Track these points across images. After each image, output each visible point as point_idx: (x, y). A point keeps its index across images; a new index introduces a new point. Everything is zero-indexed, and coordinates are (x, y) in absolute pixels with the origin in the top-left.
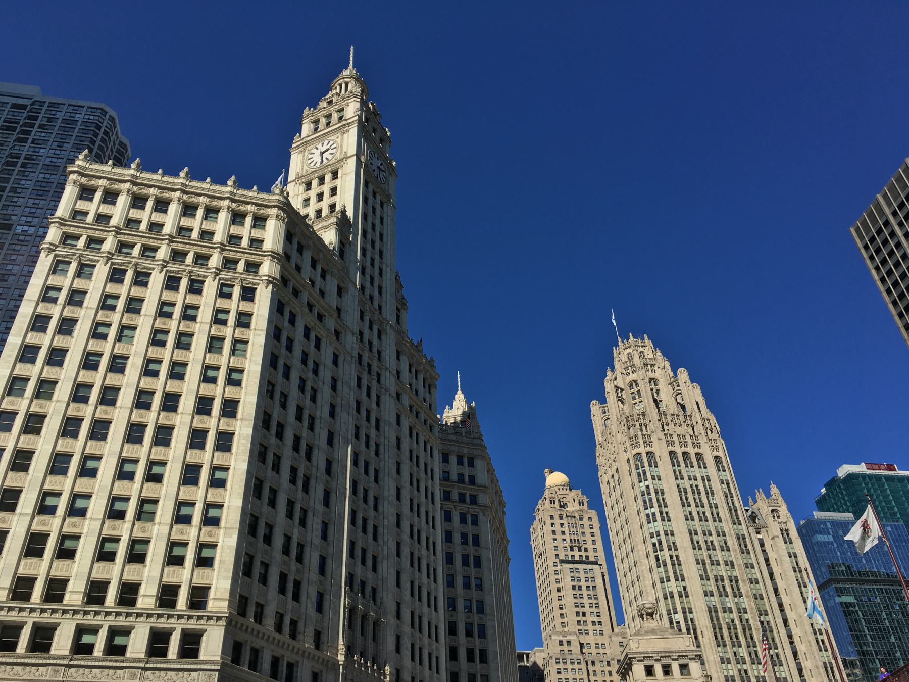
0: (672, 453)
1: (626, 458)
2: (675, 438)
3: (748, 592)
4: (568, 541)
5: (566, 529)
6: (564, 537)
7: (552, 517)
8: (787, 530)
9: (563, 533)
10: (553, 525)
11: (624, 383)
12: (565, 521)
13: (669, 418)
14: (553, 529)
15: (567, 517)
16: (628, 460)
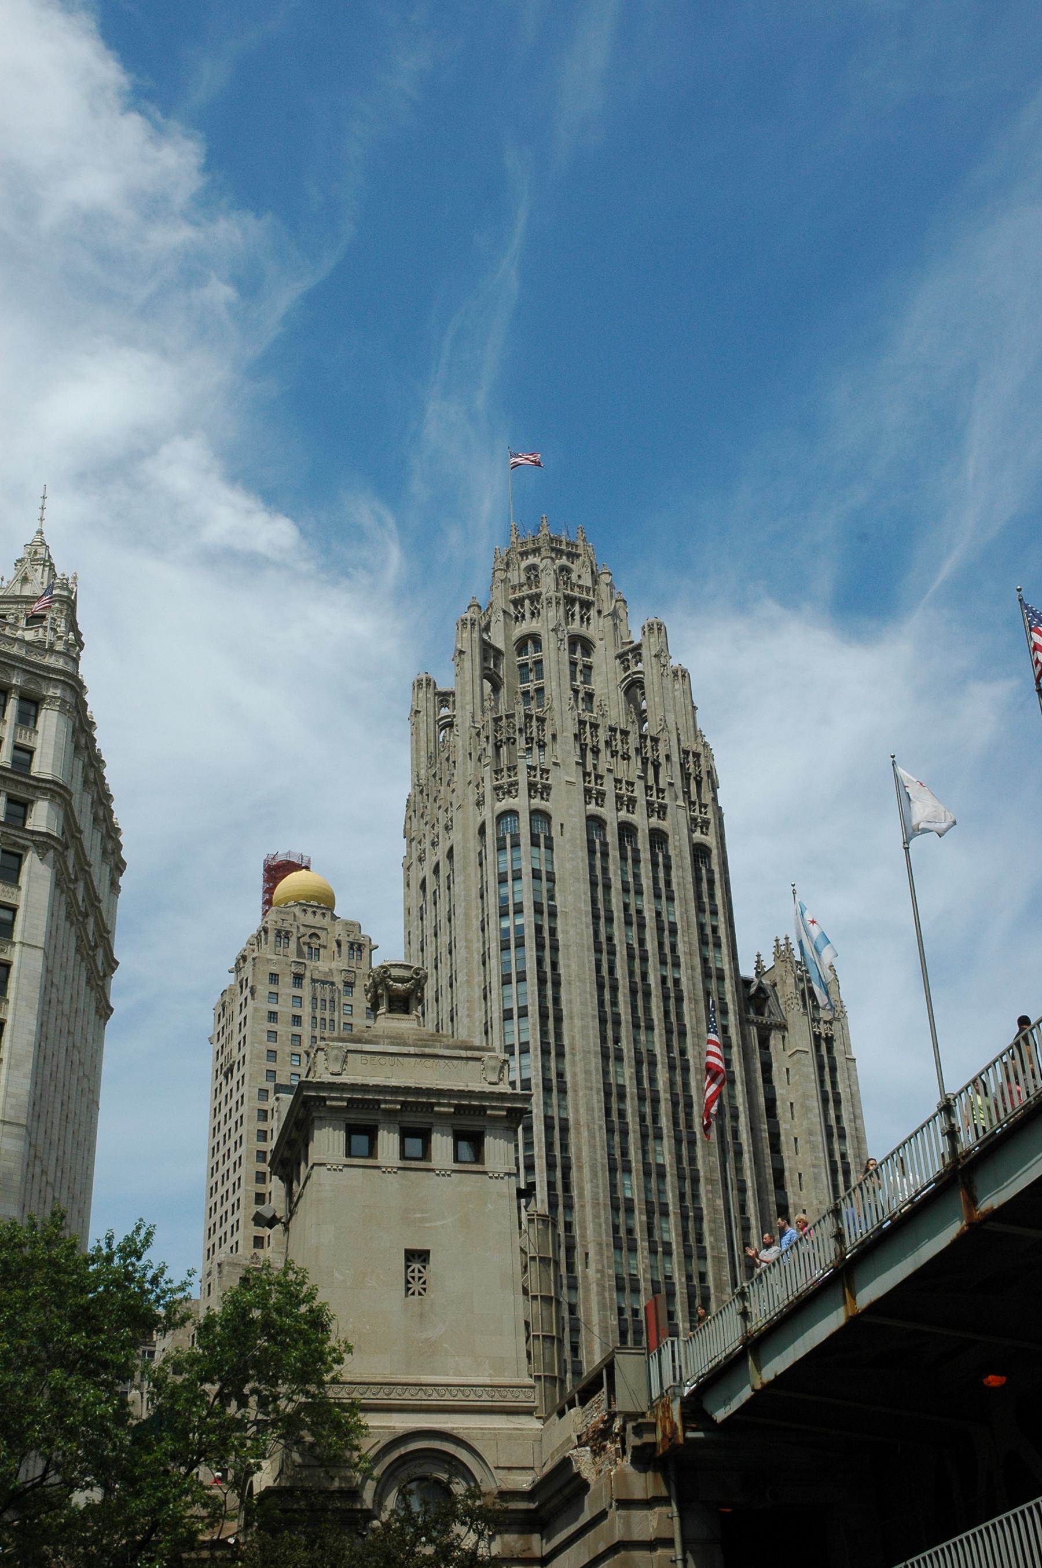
0: (595, 823)
1: (479, 820)
2: (608, 786)
3: (712, 1170)
4: (306, 1042)
5: (306, 1012)
6: (296, 1030)
7: (274, 978)
8: (830, 1040)
9: (297, 1020)
10: (274, 996)
11: (507, 637)
12: (306, 992)
13: (603, 735)
14: (274, 1008)
15: (314, 981)
16: (482, 831)
